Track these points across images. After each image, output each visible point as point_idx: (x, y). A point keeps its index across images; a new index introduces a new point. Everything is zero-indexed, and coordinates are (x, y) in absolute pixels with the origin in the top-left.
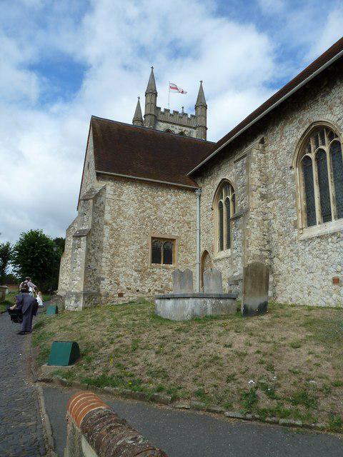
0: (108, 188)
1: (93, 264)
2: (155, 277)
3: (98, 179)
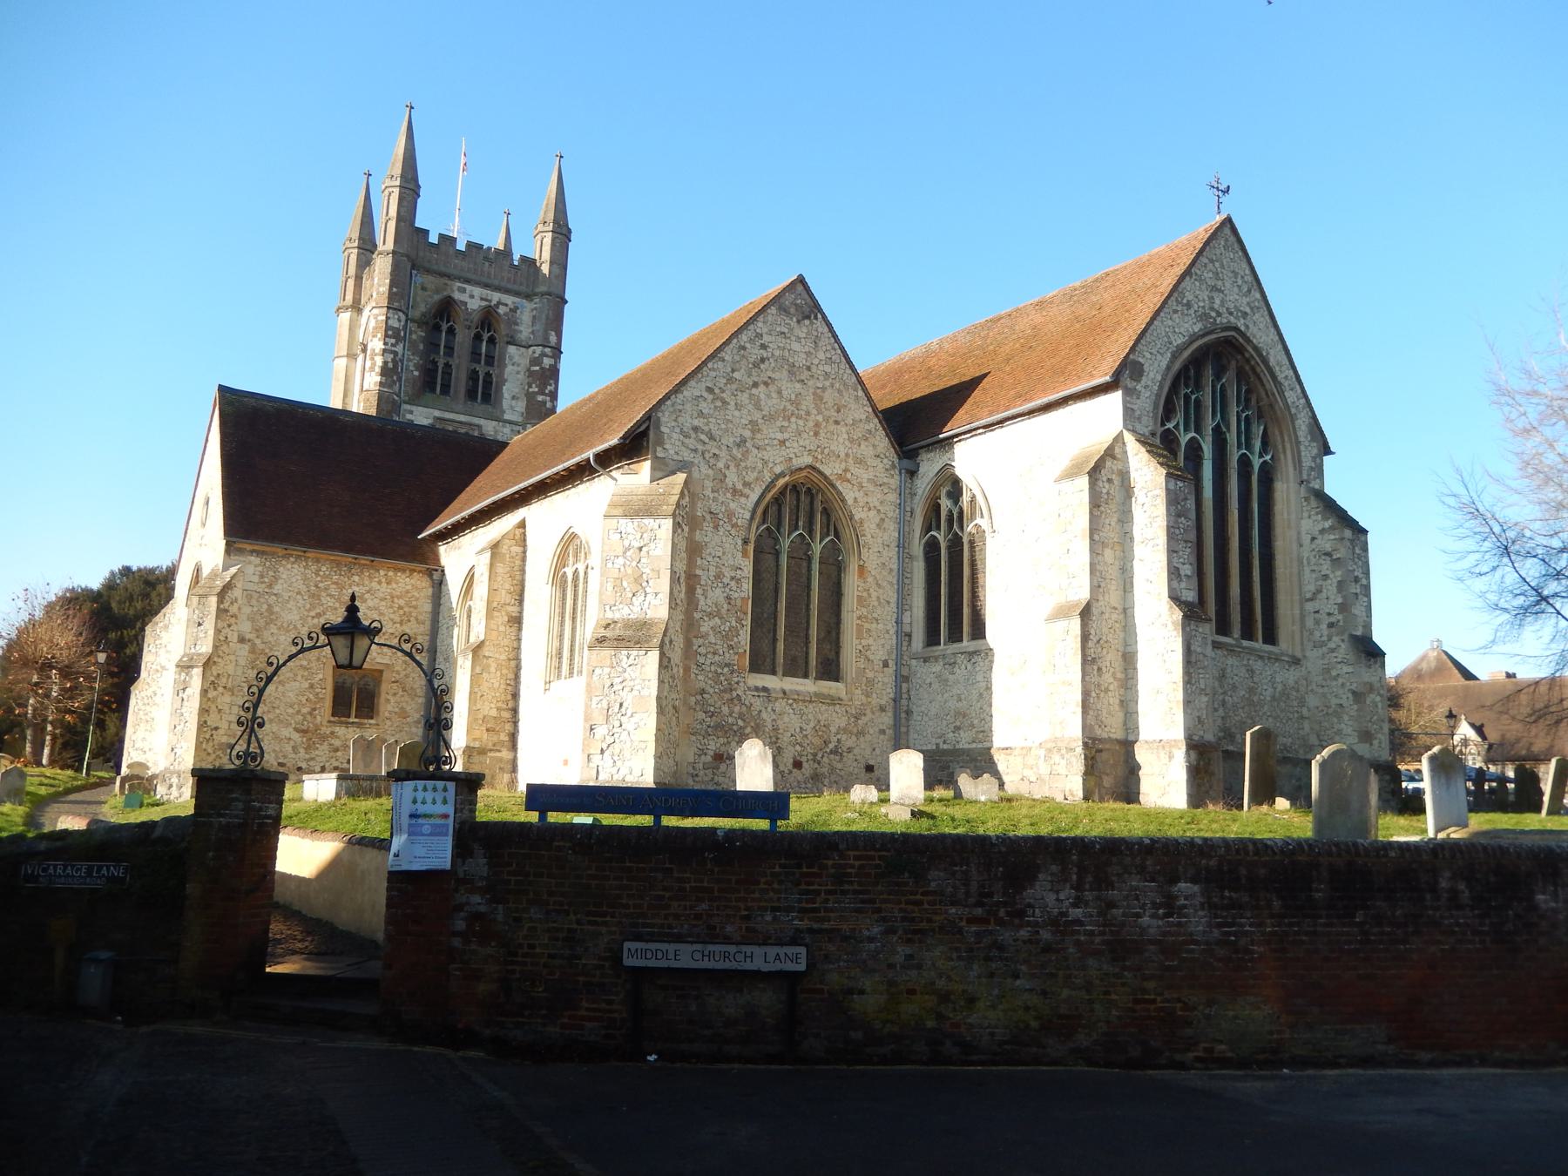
2: (337, 743)
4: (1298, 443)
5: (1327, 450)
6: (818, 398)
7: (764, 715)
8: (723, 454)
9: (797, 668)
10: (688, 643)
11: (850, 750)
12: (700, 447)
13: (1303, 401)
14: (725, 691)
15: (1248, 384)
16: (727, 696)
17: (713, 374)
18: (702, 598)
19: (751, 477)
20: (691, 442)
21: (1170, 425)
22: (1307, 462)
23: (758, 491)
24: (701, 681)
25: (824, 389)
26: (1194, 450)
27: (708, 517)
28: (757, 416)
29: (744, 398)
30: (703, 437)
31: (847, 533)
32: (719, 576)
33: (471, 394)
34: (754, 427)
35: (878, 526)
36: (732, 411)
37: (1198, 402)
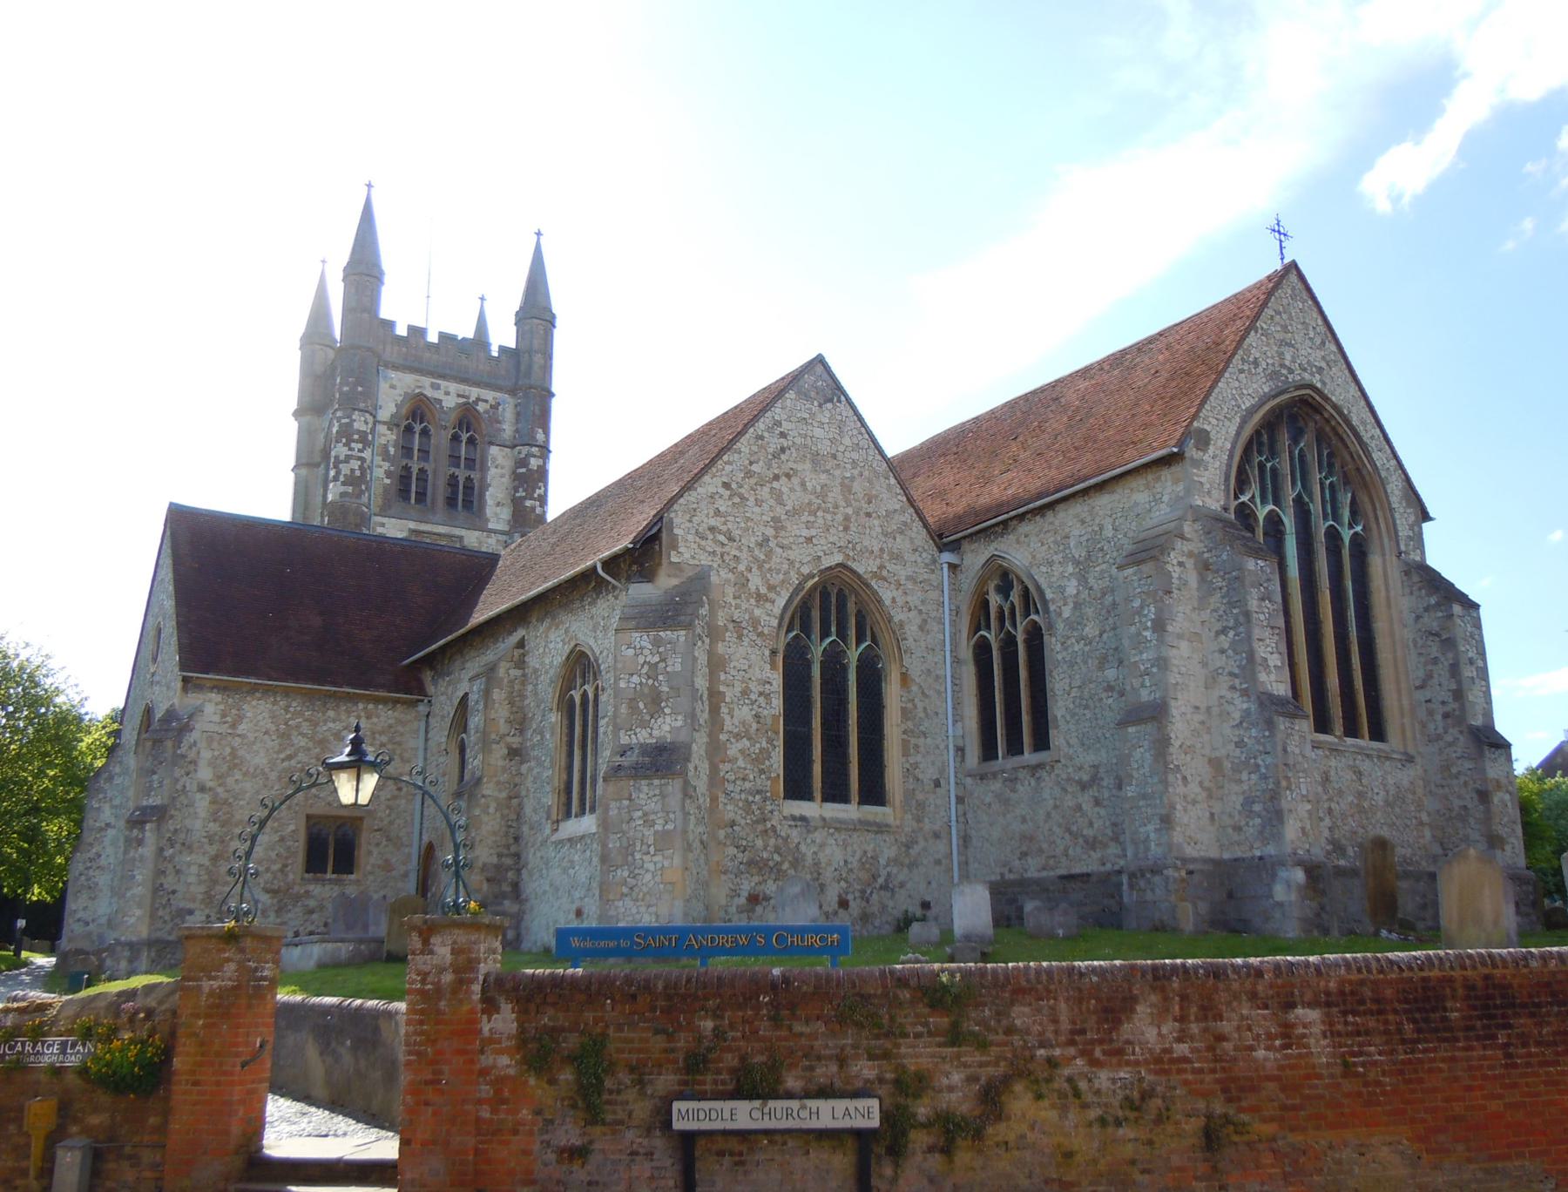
0: (209, 709)
1: (169, 881)
2: (312, 903)
3: (185, 689)
4: (1392, 510)
5: (1425, 516)
6: (846, 488)
7: (803, 848)
8: (744, 555)
9: (836, 792)
10: (714, 769)
11: (902, 885)
12: (719, 550)
13: (1394, 462)
14: (757, 822)
15: (1329, 446)
16: (760, 827)
17: (728, 468)
18: (727, 718)
19: (776, 579)
20: (710, 545)
21: (1244, 498)
22: (1404, 532)
23: (785, 595)
24: (730, 811)
25: (853, 479)
26: (1274, 522)
27: (731, 626)
28: (779, 511)
29: (765, 492)
30: (722, 538)
31: (885, 638)
32: (745, 692)
33: (451, 502)
34: (778, 525)
35: (921, 628)
36: (753, 510)
37: (1274, 470)
